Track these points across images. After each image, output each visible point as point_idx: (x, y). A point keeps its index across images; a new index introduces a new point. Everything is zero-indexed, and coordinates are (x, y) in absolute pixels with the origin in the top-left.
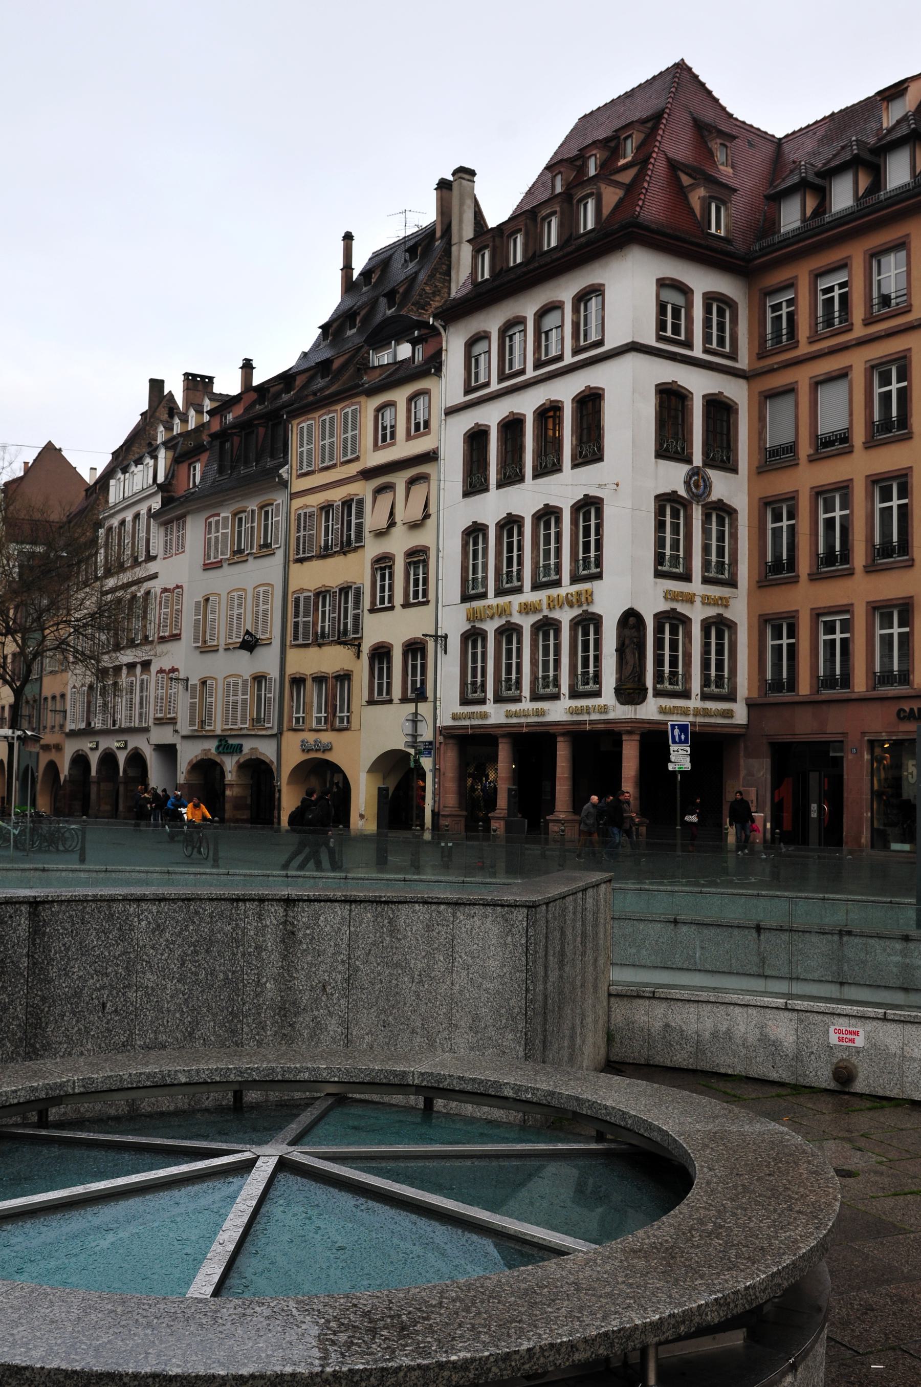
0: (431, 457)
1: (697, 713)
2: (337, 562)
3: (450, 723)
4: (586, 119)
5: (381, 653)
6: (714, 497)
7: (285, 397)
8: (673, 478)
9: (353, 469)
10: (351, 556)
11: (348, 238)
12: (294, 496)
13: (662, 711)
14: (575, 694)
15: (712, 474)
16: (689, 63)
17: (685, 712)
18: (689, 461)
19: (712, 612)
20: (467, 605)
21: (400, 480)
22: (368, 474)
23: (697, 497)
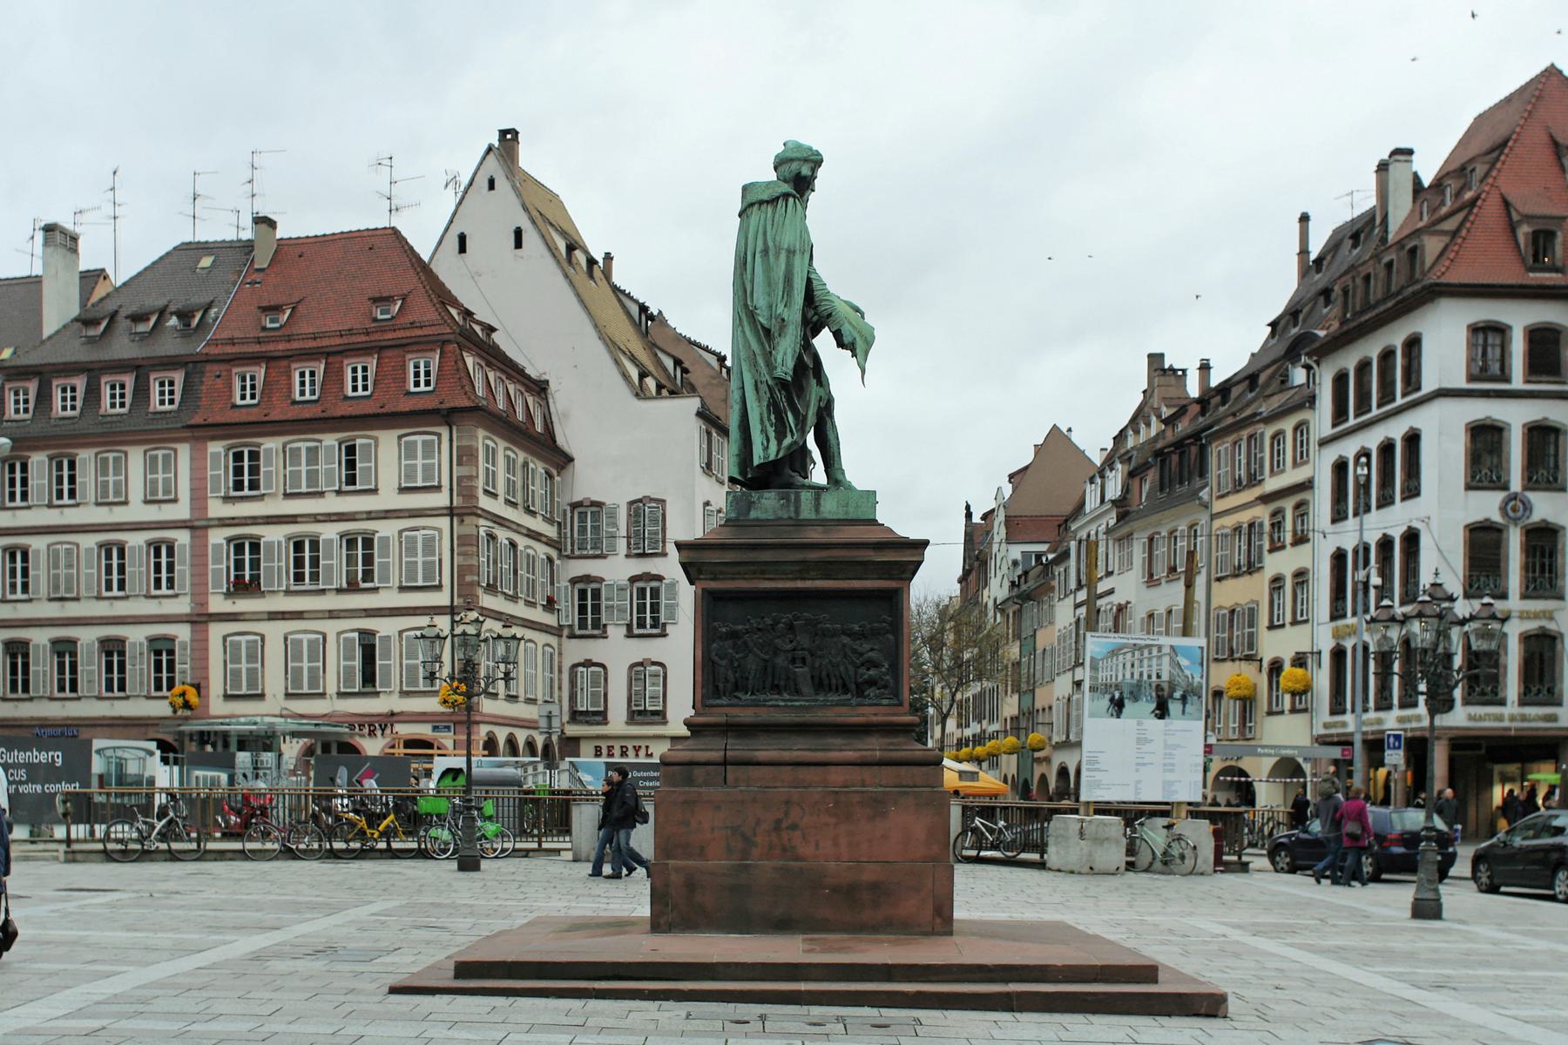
0: (1308, 485)
1: (1512, 718)
2: (1244, 581)
3: (1323, 731)
4: (1480, 119)
5: (1276, 668)
6: (1536, 517)
7: (1222, 409)
8: (1487, 506)
9: (1256, 492)
10: (1256, 575)
11: (1304, 219)
12: (1213, 517)
13: (1471, 718)
14: (1402, 706)
15: (1534, 497)
16: (1559, 66)
17: (1500, 718)
18: (1505, 487)
19: (1532, 626)
20: (1334, 624)
21: (1288, 505)
22: (1265, 499)
23: (1515, 521)
